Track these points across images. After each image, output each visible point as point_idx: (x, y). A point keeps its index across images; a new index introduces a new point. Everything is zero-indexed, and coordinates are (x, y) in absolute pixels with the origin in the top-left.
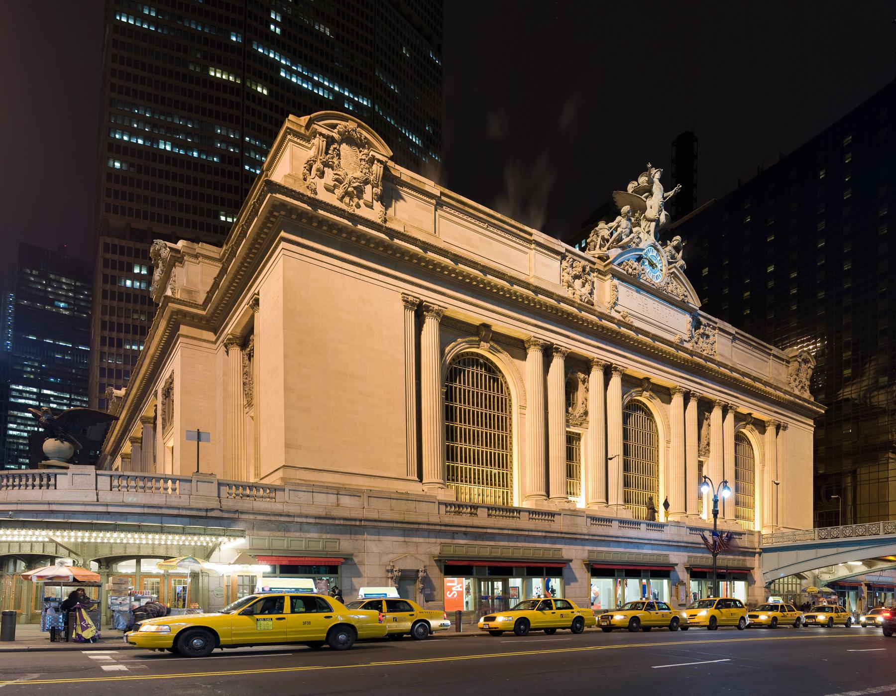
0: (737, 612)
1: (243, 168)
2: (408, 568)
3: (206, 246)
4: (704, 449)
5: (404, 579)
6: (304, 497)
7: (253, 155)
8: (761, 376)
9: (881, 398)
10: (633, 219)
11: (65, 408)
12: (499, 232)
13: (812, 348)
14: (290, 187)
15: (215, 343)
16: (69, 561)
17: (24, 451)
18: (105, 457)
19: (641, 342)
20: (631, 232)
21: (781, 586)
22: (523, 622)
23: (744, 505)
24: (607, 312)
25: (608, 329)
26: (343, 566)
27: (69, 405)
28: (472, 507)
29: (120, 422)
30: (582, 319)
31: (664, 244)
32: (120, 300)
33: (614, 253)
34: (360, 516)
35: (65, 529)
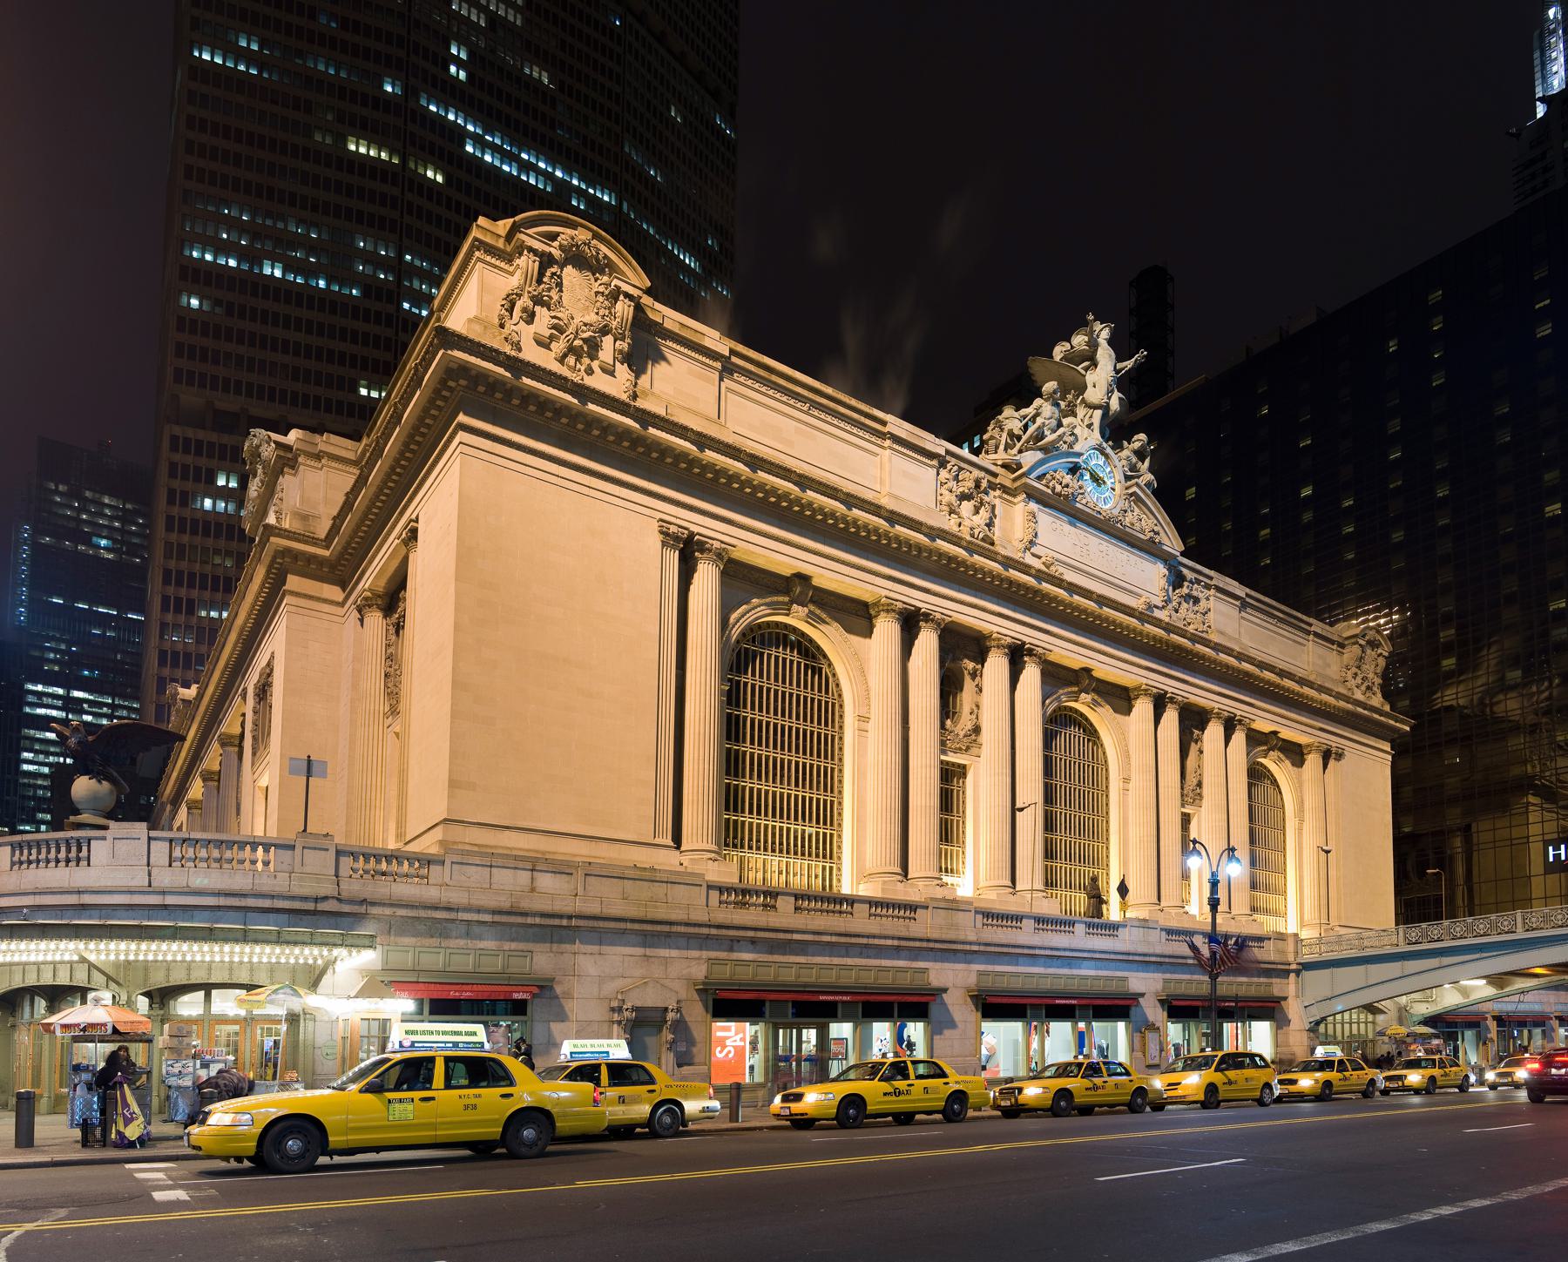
0: (1258, 1076)
1: (400, 306)
2: (649, 1004)
3: (334, 439)
4: (1191, 792)
5: (641, 1024)
6: (476, 875)
7: (416, 284)
8: (1292, 669)
9: (1511, 706)
10: (1063, 404)
11: (105, 722)
12: (829, 418)
13: (1384, 622)
14: (477, 339)
15: (342, 604)
16: (106, 996)
17: (43, 799)
18: (163, 805)
19: (1077, 608)
20: (1060, 425)
21: (1339, 1027)
22: (853, 1102)
23: (1267, 889)
24: (1017, 556)
25: (1020, 585)
26: (536, 1001)
27: (110, 717)
28: (766, 893)
29: (187, 744)
30: (973, 566)
31: (1118, 447)
32: (194, 532)
33: (1029, 458)
34: (569, 910)
35: (101, 938)
